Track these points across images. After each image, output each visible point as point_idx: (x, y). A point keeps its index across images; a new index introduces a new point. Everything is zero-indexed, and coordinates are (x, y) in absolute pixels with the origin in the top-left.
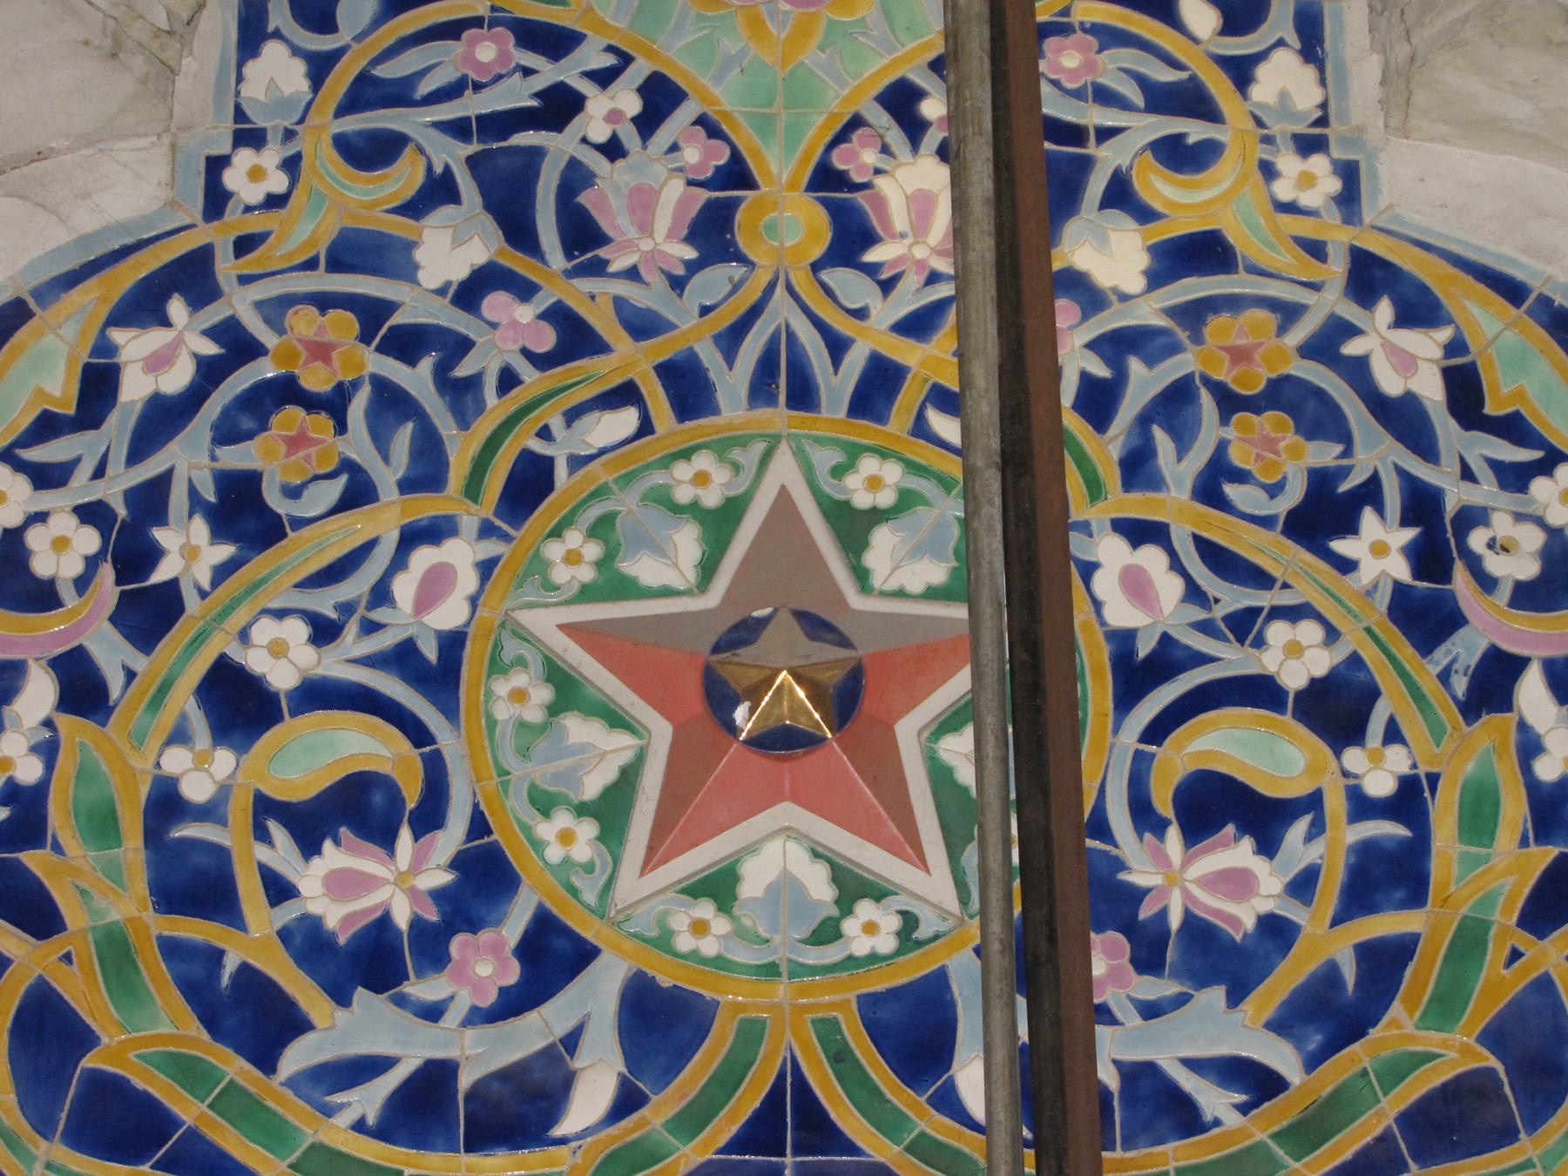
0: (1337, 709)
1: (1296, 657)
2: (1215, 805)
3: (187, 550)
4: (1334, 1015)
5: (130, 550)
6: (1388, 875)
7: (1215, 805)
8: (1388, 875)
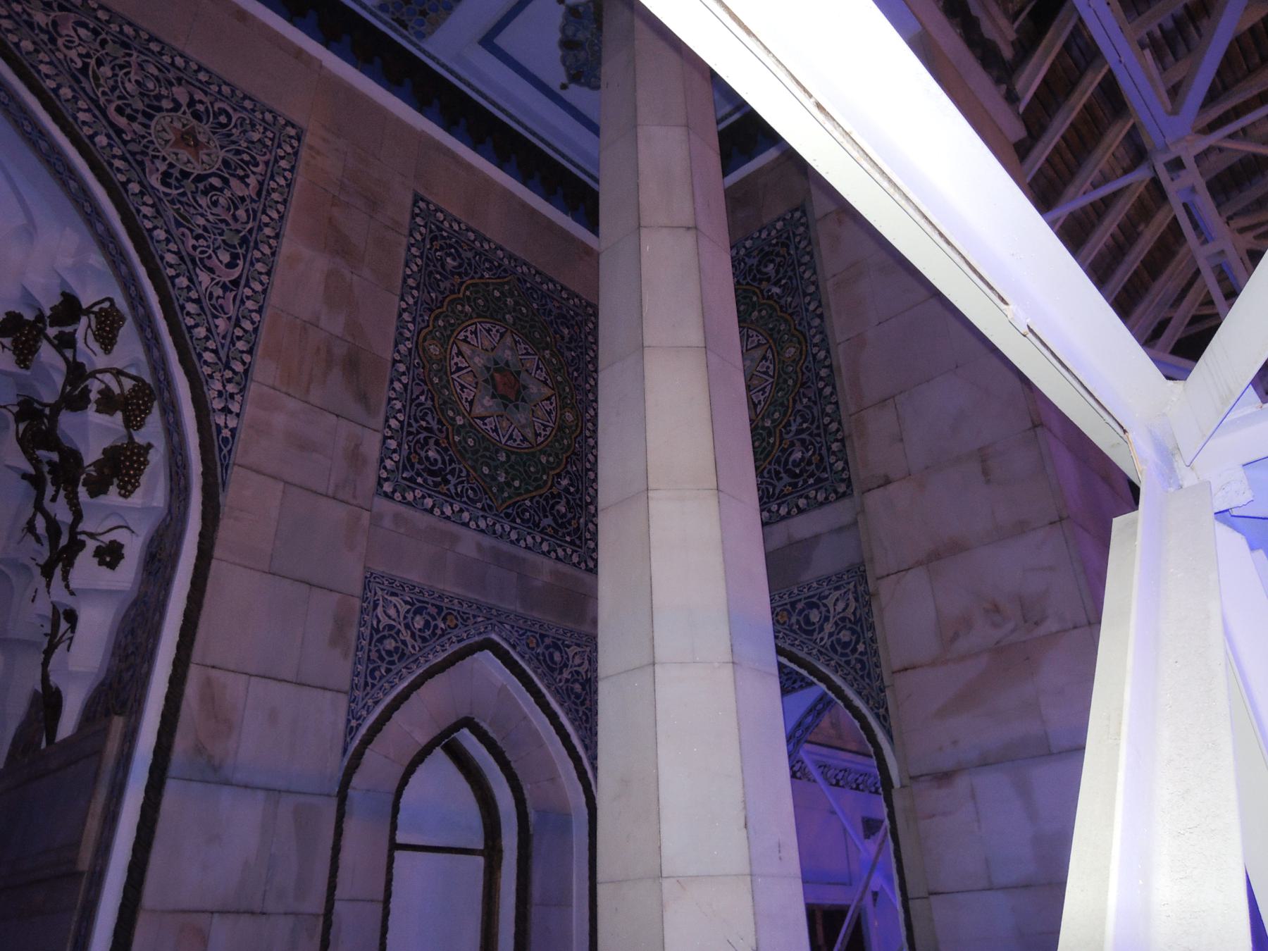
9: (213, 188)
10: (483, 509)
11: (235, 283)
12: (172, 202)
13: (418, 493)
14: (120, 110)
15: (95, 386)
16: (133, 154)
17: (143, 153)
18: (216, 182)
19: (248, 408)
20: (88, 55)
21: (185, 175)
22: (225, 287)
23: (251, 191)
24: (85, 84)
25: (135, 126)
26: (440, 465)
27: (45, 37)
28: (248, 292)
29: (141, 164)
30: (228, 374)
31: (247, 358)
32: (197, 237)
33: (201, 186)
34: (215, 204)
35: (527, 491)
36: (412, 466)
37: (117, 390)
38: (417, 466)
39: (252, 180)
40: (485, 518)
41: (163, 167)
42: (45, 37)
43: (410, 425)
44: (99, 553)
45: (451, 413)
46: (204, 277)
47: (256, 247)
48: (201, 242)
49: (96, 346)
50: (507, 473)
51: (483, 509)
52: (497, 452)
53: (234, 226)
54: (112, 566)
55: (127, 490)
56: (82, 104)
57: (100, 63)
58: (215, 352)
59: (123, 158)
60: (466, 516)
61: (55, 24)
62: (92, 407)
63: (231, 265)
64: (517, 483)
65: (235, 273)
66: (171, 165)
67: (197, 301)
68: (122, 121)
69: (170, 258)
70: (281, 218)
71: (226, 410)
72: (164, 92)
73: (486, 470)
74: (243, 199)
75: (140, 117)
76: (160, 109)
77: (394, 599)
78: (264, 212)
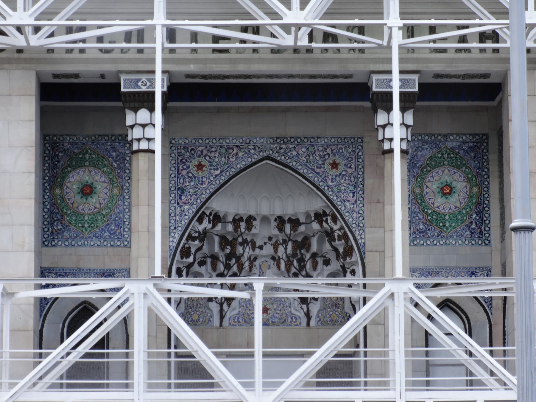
0: (280, 310)
1: (279, 309)
2: (277, 313)
3: (248, 305)
4: (280, 319)
5: (246, 305)
6: (282, 315)
7: (277, 313)
8: (282, 315)
9: (343, 175)
10: (441, 237)
11: (356, 201)
12: (335, 187)
13: (418, 241)
14: (317, 167)
15: (336, 235)
16: (323, 178)
17: (325, 176)
18: (344, 173)
19: (366, 236)
20: (306, 156)
21: (336, 176)
22: (353, 204)
23: (354, 170)
24: (308, 165)
25: (322, 170)
26: (424, 229)
27: (297, 158)
28: (359, 202)
29: (326, 180)
30: (359, 228)
31: (363, 221)
32: (343, 194)
33: (341, 177)
34: (345, 180)
35: (458, 225)
36: (415, 233)
37: (340, 234)
38: (417, 232)
39: (353, 166)
40: (442, 240)
41: (330, 177)
42: (297, 158)
43: (412, 220)
44: (351, 272)
45: (426, 210)
46: (348, 204)
47: (358, 187)
48: (345, 194)
49: (333, 223)
50: (449, 222)
51: (441, 237)
52: (445, 216)
53: (351, 184)
54: (354, 275)
55: (351, 256)
56: (309, 172)
57: (309, 156)
58: (355, 223)
59: (322, 181)
60: (435, 242)
61: (297, 153)
62: (337, 241)
63: (353, 196)
64: (453, 224)
65: (355, 198)
66: (333, 175)
67: (348, 212)
68: (318, 170)
69: (339, 203)
70: (363, 173)
71: (361, 238)
72: (325, 153)
73: (441, 224)
74: (352, 174)
75: (323, 166)
76: (325, 160)
77: (414, 274)
78: (358, 174)
